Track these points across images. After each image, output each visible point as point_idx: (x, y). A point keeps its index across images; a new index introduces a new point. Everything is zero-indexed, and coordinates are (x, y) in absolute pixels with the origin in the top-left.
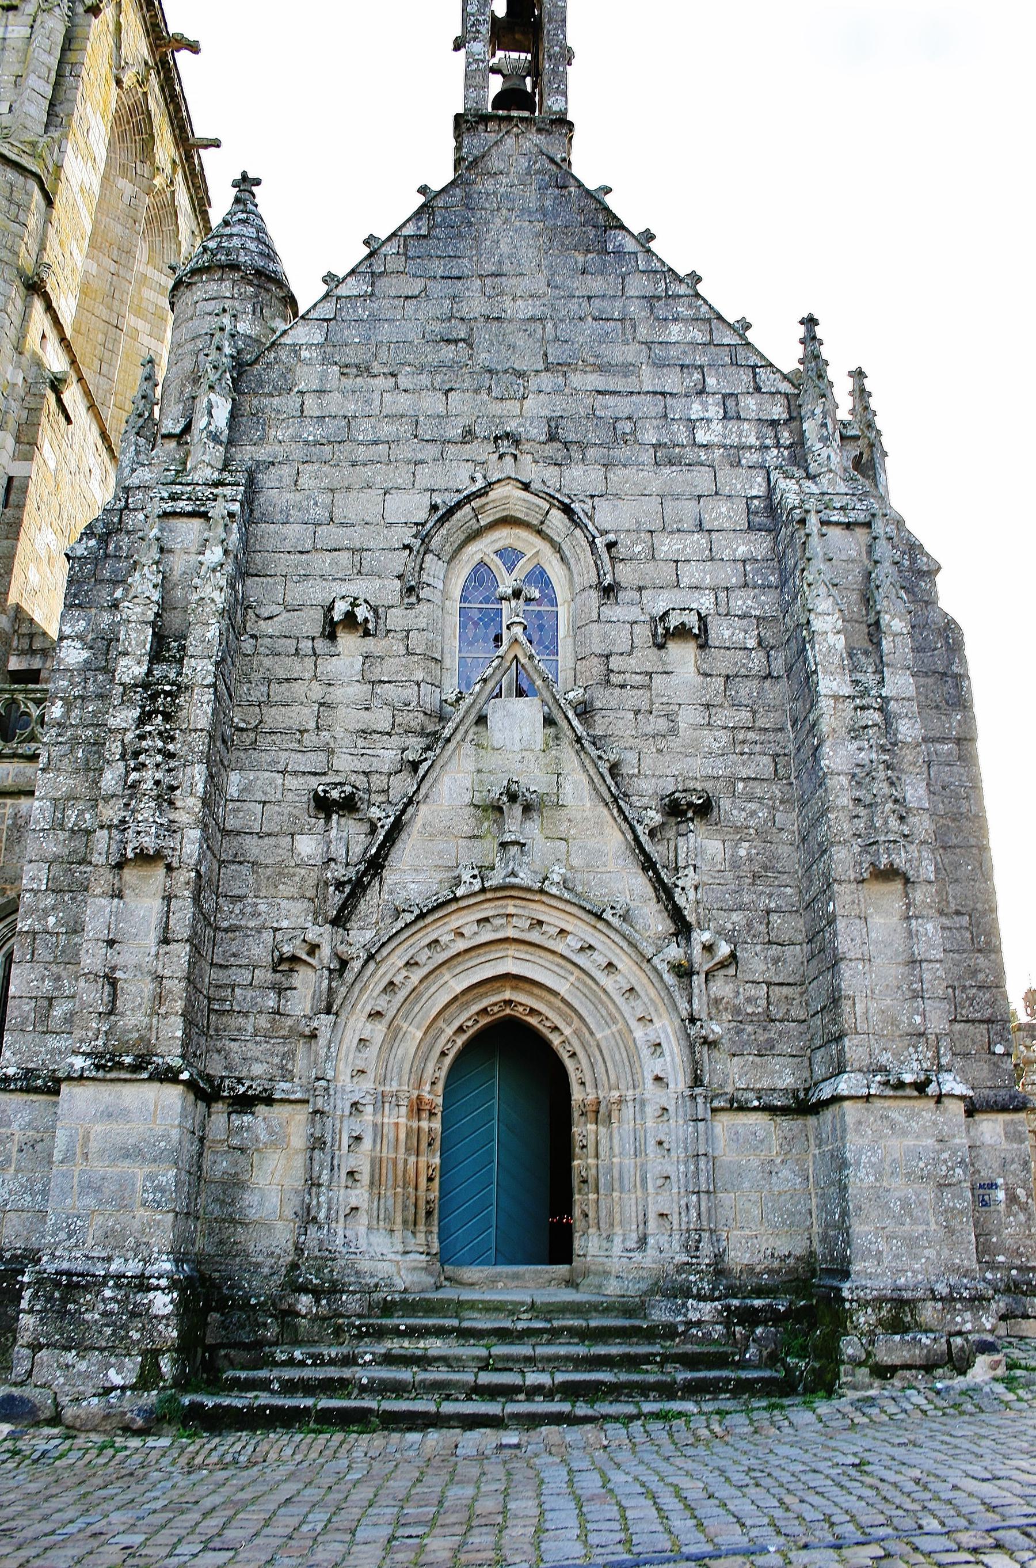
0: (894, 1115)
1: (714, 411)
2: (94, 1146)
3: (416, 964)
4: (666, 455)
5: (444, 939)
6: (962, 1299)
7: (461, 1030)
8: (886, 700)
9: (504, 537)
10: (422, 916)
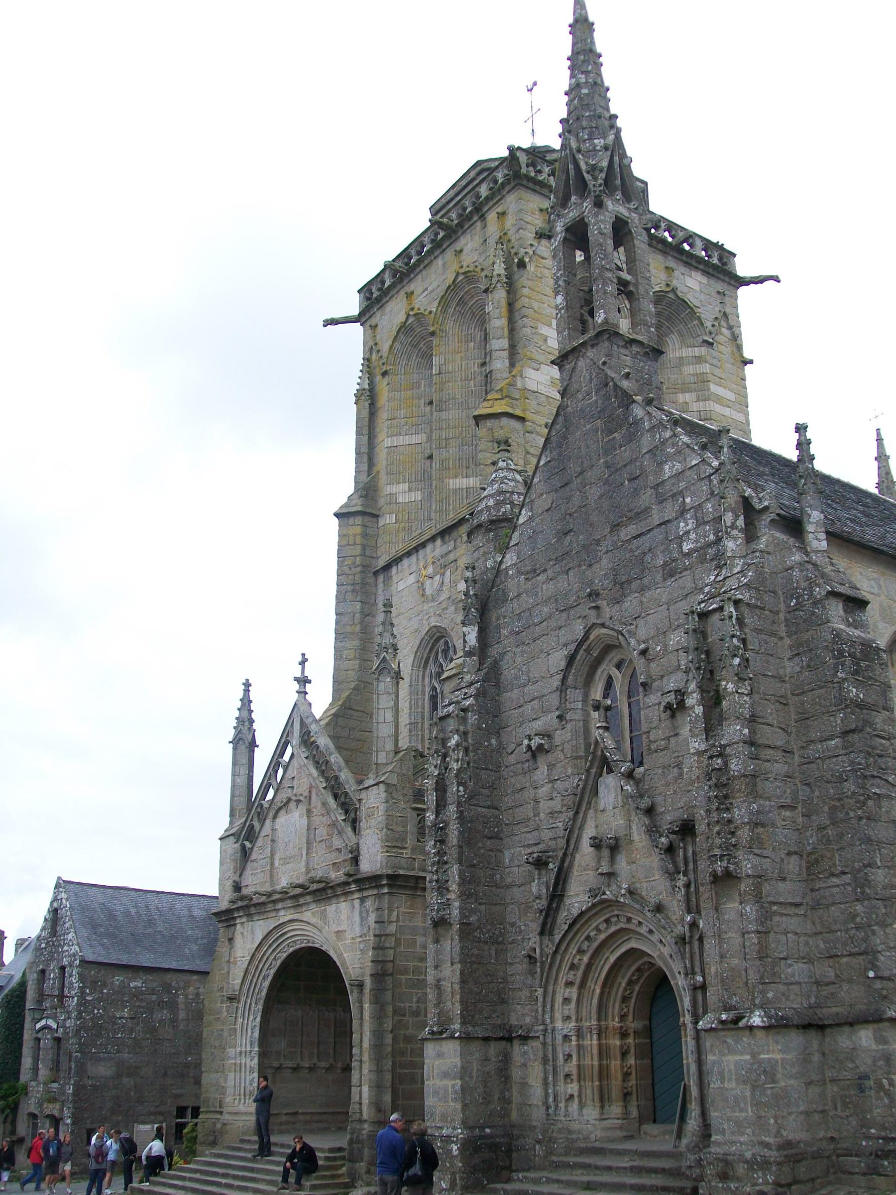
0: (729, 1040)
3: (584, 951)
4: (670, 571)
5: (592, 934)
6: (757, 1164)
7: (630, 983)
8: (725, 746)
10: (571, 925)
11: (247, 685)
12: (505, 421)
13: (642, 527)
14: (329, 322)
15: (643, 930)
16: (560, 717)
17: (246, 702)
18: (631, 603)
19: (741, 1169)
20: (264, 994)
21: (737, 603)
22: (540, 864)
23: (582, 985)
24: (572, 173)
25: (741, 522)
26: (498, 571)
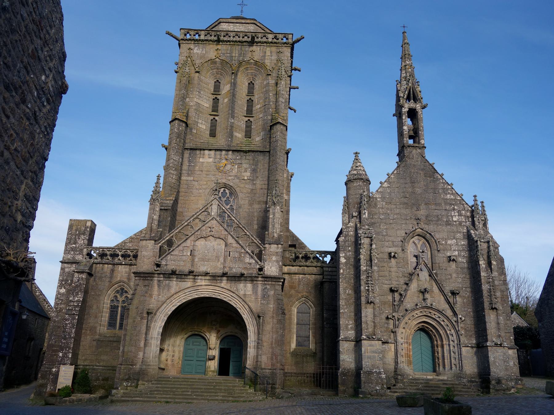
1: (456, 214)
2: (369, 351)
4: (448, 223)
14: (168, 33)
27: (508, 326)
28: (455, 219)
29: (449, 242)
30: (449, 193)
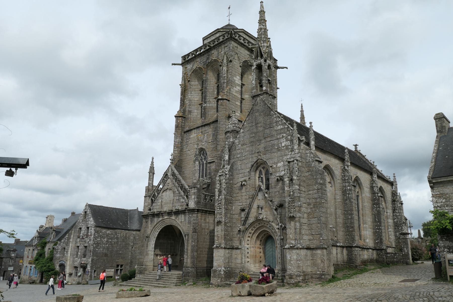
1: (285, 140)
4: (279, 150)
7: (262, 237)
9: (262, 166)
11: (153, 158)
12: (225, 101)
13: (272, 139)
14: (173, 64)
15: (268, 226)
16: (249, 178)
17: (152, 163)
18: (268, 156)
19: (294, 277)
20: (156, 236)
21: (297, 160)
22: (243, 210)
23: (252, 237)
24: (259, 52)
25: (297, 143)
26: (233, 143)
27: (319, 229)
28: (283, 145)
29: (279, 165)
30: (280, 125)
